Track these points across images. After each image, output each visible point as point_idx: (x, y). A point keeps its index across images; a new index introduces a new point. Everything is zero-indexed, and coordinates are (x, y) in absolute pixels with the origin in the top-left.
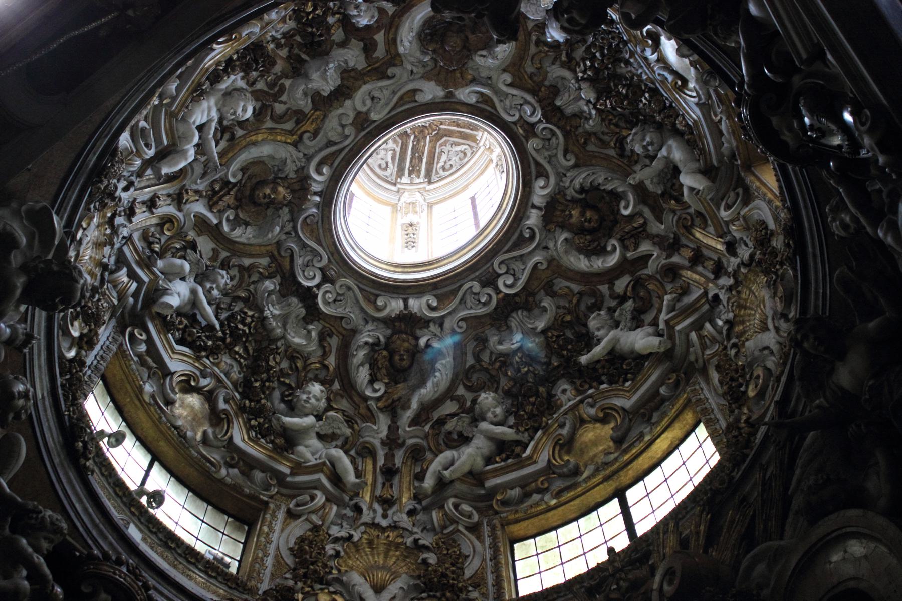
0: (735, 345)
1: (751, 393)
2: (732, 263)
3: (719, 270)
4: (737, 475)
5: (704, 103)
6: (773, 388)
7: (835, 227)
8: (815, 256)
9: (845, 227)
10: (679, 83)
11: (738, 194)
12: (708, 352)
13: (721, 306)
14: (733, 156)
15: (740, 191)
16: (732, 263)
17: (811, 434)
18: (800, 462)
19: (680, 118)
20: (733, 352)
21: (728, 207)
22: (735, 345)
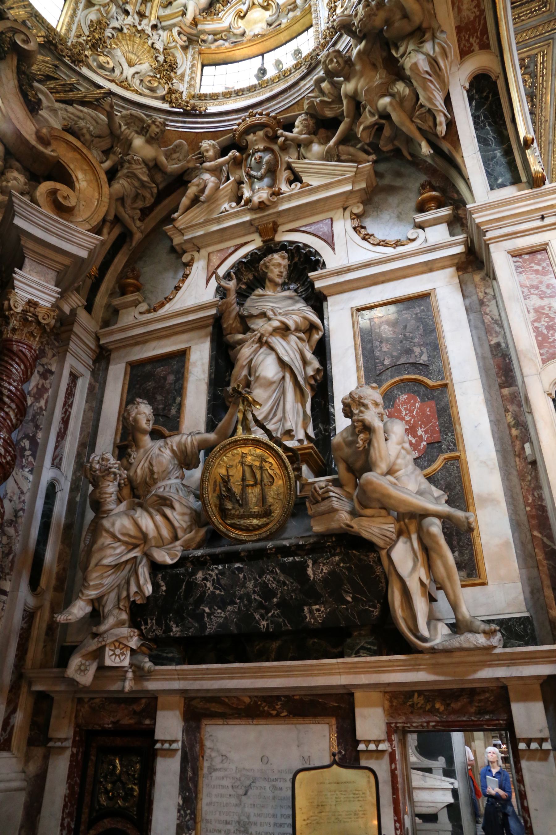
0: (113, 35)
1: (102, 59)
2: (145, 25)
3: (142, 15)
4: (67, 60)
5: (230, 28)
6: (106, 75)
7: (206, 144)
8: (185, 122)
9: (207, 151)
10: (242, 15)
11: (185, 42)
12: (102, 9)
13: (123, 16)
14: (204, 41)
15: (187, 43)
16: (145, 25)
17: (106, 119)
18: (90, 111)
19: (222, 8)
20: (110, 35)
21: (179, 33)
22: (113, 35)
